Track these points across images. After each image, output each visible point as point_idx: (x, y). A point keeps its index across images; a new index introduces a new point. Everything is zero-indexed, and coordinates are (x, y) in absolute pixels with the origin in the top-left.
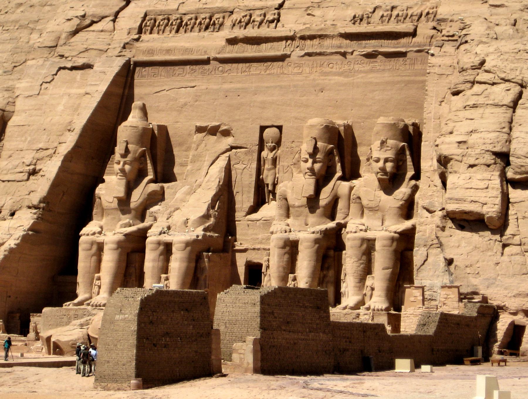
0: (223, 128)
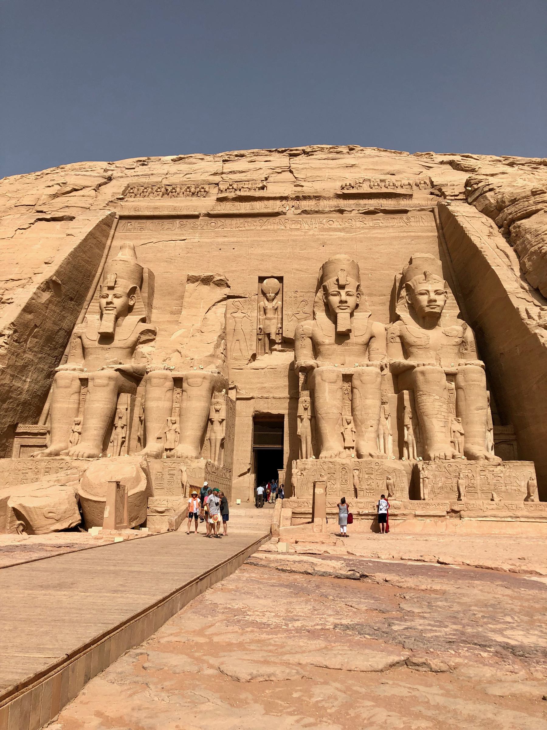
0: (219, 278)
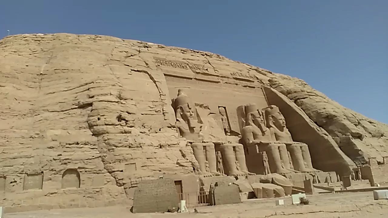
0: (205, 105)
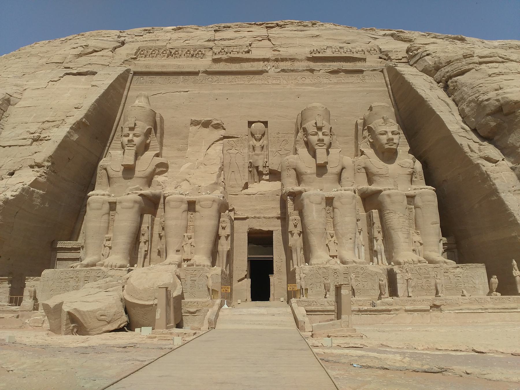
0: (216, 122)
